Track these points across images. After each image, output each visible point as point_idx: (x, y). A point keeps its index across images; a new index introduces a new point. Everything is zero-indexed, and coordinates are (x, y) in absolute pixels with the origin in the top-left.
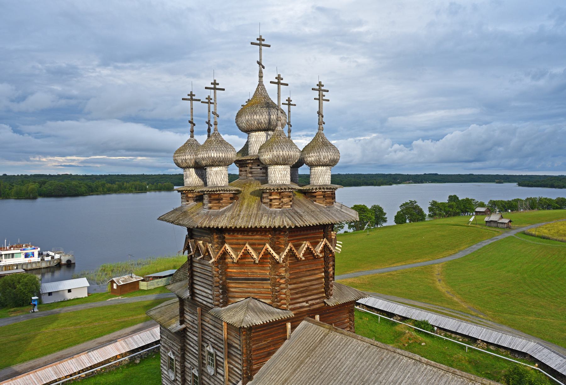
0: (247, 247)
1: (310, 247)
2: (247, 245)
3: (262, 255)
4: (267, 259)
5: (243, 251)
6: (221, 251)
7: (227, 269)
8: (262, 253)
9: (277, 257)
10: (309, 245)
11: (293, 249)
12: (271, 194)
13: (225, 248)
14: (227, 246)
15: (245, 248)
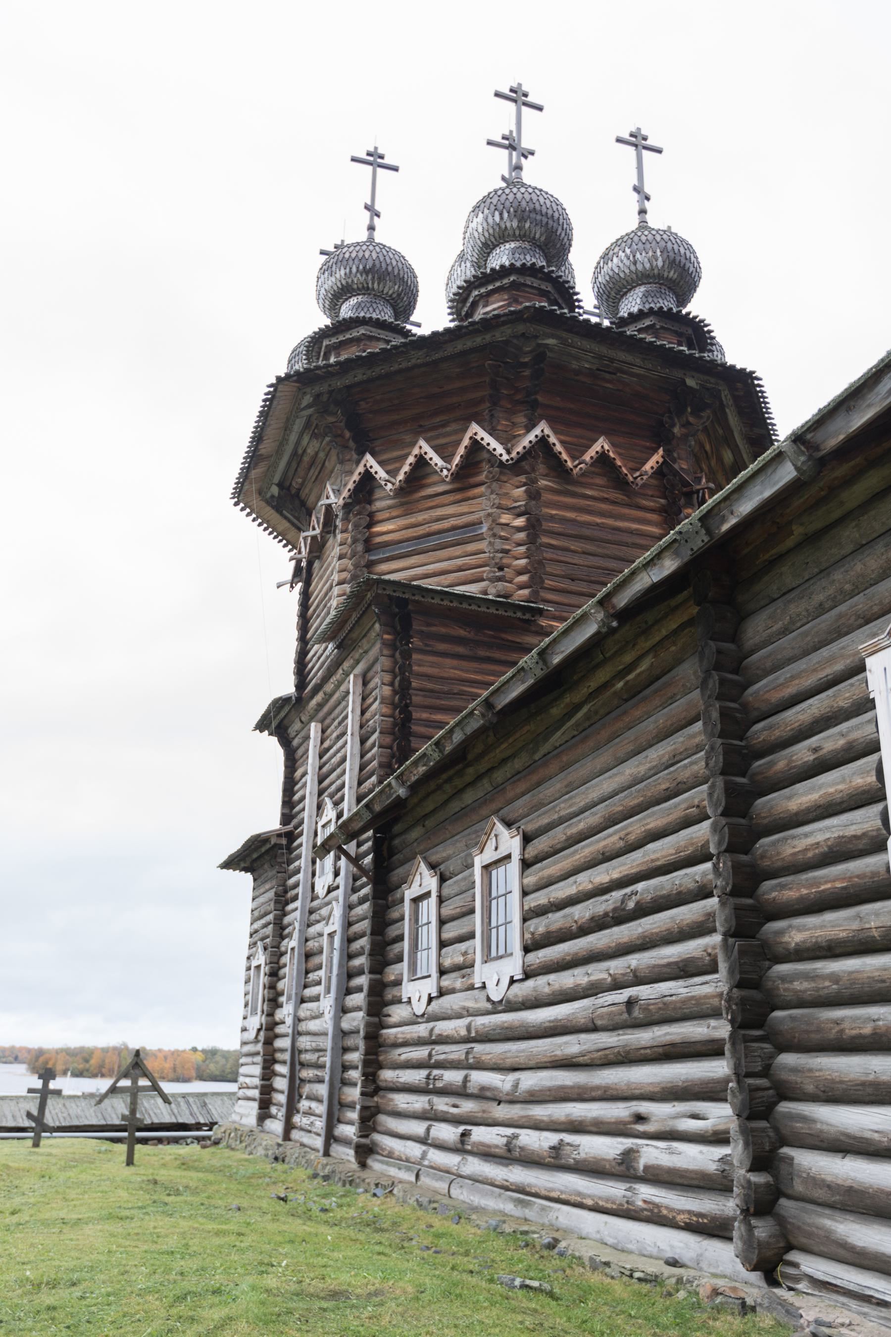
0: (421, 447)
1: (611, 454)
2: (422, 442)
3: (461, 456)
4: (478, 473)
5: (411, 459)
6: (356, 477)
7: (370, 526)
8: (461, 451)
9: (500, 449)
10: (606, 447)
11: (553, 439)
12: (487, 301)
13: (365, 466)
14: (369, 460)
15: (416, 451)
